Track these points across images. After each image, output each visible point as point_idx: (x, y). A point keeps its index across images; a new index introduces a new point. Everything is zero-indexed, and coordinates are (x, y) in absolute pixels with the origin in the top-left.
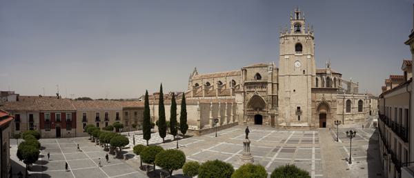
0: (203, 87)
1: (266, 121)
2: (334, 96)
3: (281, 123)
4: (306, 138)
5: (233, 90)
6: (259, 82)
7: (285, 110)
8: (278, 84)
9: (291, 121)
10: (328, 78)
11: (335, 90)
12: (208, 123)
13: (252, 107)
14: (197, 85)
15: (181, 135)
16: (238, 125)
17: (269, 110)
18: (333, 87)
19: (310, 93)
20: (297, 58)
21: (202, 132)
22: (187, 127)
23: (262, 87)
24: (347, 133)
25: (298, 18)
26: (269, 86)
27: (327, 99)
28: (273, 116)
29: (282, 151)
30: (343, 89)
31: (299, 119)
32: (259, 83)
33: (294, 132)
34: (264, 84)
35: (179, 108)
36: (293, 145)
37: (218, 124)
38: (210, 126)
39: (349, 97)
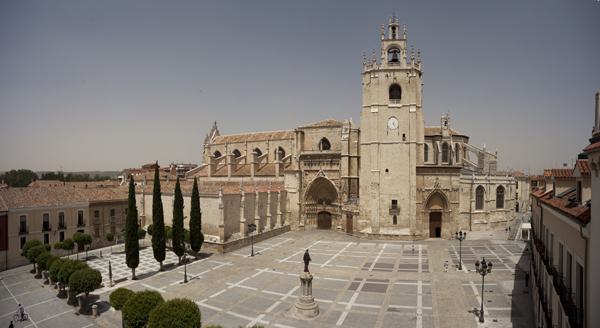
0: (229, 159)
1: (338, 224)
2: (455, 180)
3: (363, 228)
4: (410, 259)
5: (281, 166)
6: (327, 154)
7: (371, 207)
8: (359, 158)
9: (381, 225)
10: (445, 146)
11: (457, 169)
12: (238, 230)
13: (314, 198)
14: (218, 154)
15: (191, 254)
16: (289, 230)
17: (343, 204)
18: (455, 164)
19: (414, 177)
20: (392, 112)
21: (227, 246)
22: (201, 238)
23: (332, 163)
24: (477, 265)
25: (394, 36)
26: (344, 162)
28: (350, 216)
29: (367, 288)
30: (468, 165)
31: (395, 221)
32: (326, 156)
33: (385, 245)
34: (335, 158)
35: (187, 202)
36: (384, 275)
37: (256, 233)
38: (240, 235)
39: (481, 180)
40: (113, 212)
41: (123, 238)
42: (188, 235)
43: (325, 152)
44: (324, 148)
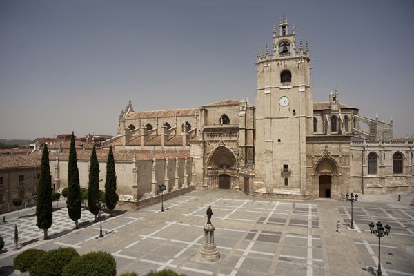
0: (142, 131)
1: (237, 184)
2: (345, 148)
3: (258, 188)
4: (298, 215)
5: (187, 137)
6: (226, 127)
7: (265, 170)
8: (254, 130)
9: (274, 186)
10: (334, 118)
11: (347, 139)
12: (150, 190)
13: (215, 163)
14: (132, 127)
15: (106, 212)
16: (195, 189)
17: (240, 168)
18: (344, 133)
19: (304, 145)
21: (140, 204)
22: (116, 198)
23: (231, 135)
24: (372, 225)
25: (284, 33)
26: (242, 134)
27: (332, 153)
28: (246, 178)
29: (261, 238)
30: (359, 134)
31: (286, 183)
32: (226, 129)
33: (278, 203)
34: (234, 131)
35: (103, 168)
36: (277, 228)
37: (165, 192)
38: (152, 194)
39: (373, 147)
40: (21, 178)
41: (33, 201)
42: (104, 195)
43: (225, 126)
44: (224, 123)
